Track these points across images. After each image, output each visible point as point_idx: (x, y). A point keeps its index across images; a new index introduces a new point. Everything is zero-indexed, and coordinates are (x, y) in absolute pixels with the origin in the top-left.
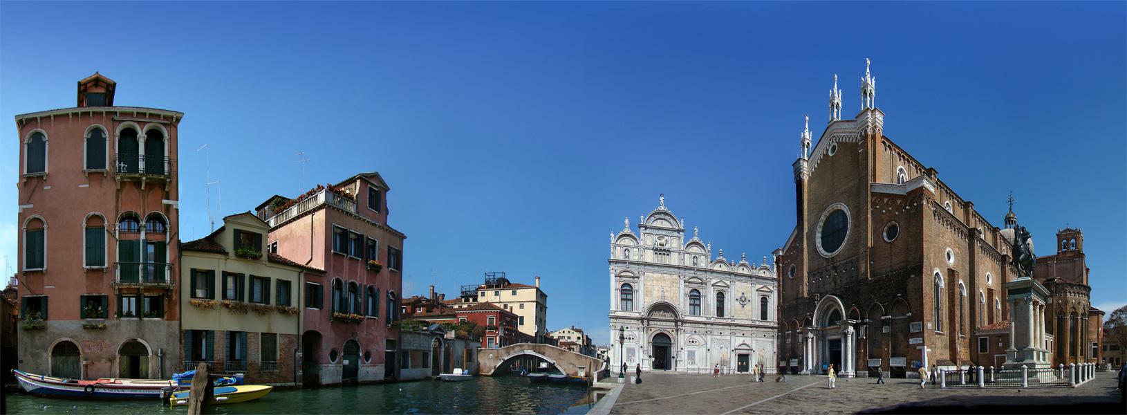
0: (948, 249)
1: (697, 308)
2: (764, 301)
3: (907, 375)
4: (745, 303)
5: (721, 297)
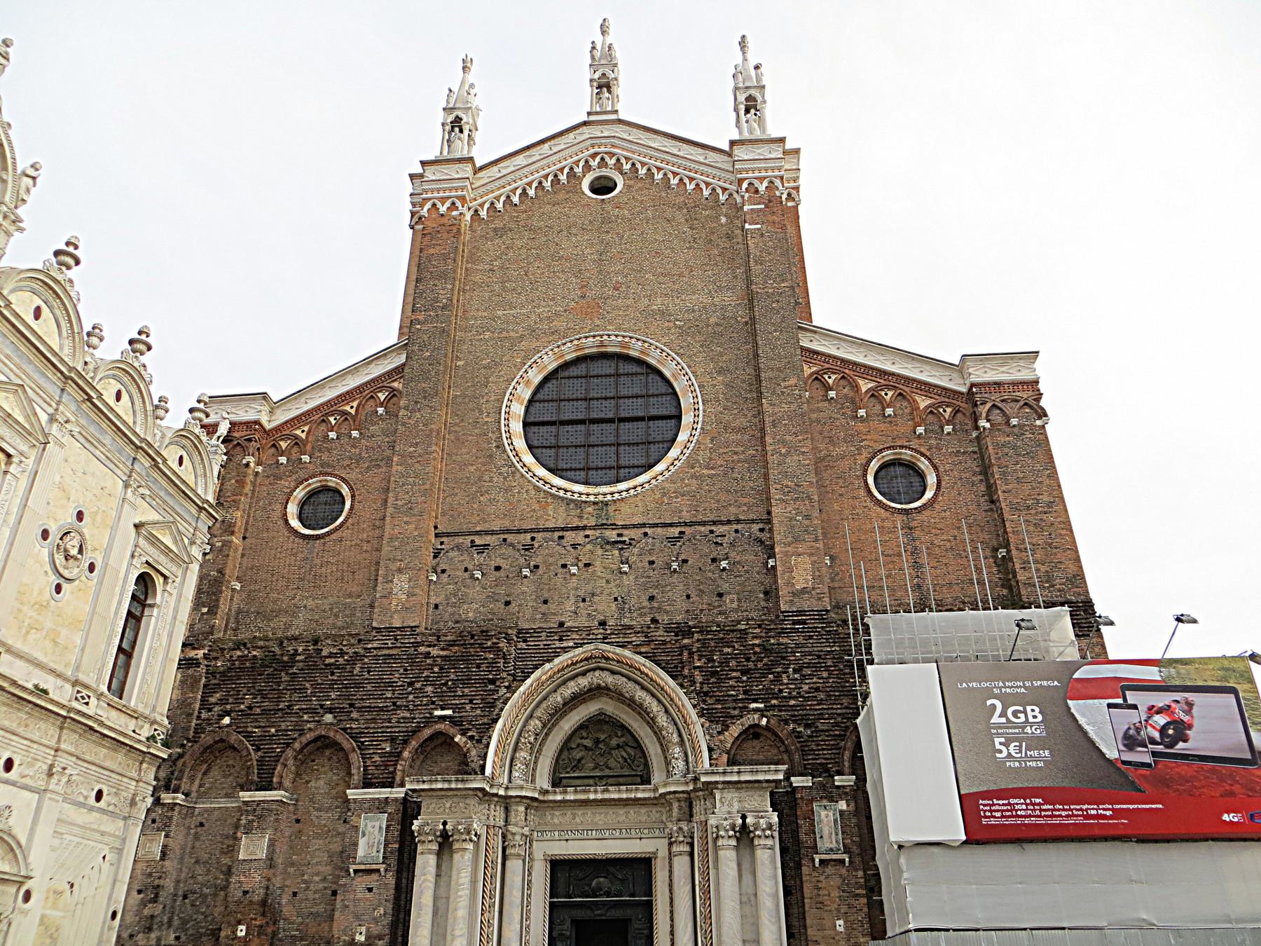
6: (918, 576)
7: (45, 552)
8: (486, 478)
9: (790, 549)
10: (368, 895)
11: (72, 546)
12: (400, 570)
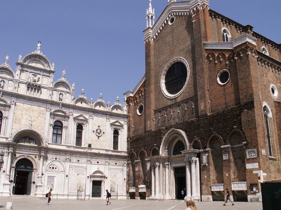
0: (272, 85)
1: (59, 138)
2: (116, 133)
3: (249, 199)
4: (100, 135)
5: (80, 128)
8: (160, 98)
9: (200, 101)
10: (149, 175)
11: (99, 131)
12: (148, 120)
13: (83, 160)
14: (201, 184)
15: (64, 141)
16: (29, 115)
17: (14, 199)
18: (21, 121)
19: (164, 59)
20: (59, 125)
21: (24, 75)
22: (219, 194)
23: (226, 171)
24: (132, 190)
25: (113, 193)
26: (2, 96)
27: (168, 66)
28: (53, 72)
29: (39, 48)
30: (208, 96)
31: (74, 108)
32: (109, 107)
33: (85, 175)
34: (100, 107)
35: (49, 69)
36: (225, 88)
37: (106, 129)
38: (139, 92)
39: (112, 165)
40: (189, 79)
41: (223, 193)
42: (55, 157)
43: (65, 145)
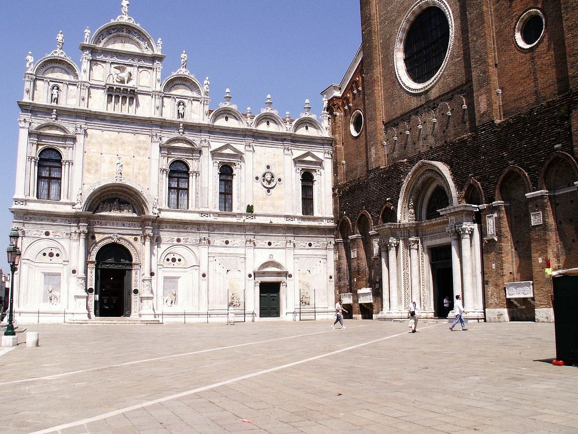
1: (183, 197)
2: (307, 179)
4: (273, 184)
5: (226, 173)
6: (535, 86)
7: (259, 184)
11: (268, 177)
12: (372, 145)
13: (238, 240)
14: (485, 283)
15: (194, 202)
16: (115, 152)
17: (92, 326)
18: (101, 168)
19: (398, 5)
20: (180, 169)
21: (99, 70)
22: (524, 305)
23: (537, 250)
24: (347, 300)
25: (307, 306)
26: (56, 119)
27: (408, 21)
28: (160, 58)
29: (126, 10)
30: (495, 78)
31: (212, 130)
32: (288, 123)
33: (243, 272)
34: (268, 124)
35: (149, 52)
36: (535, 55)
37: (284, 173)
38: (352, 87)
39: (302, 249)
40: (454, 45)
41: (532, 302)
42: (176, 238)
43: (197, 210)
